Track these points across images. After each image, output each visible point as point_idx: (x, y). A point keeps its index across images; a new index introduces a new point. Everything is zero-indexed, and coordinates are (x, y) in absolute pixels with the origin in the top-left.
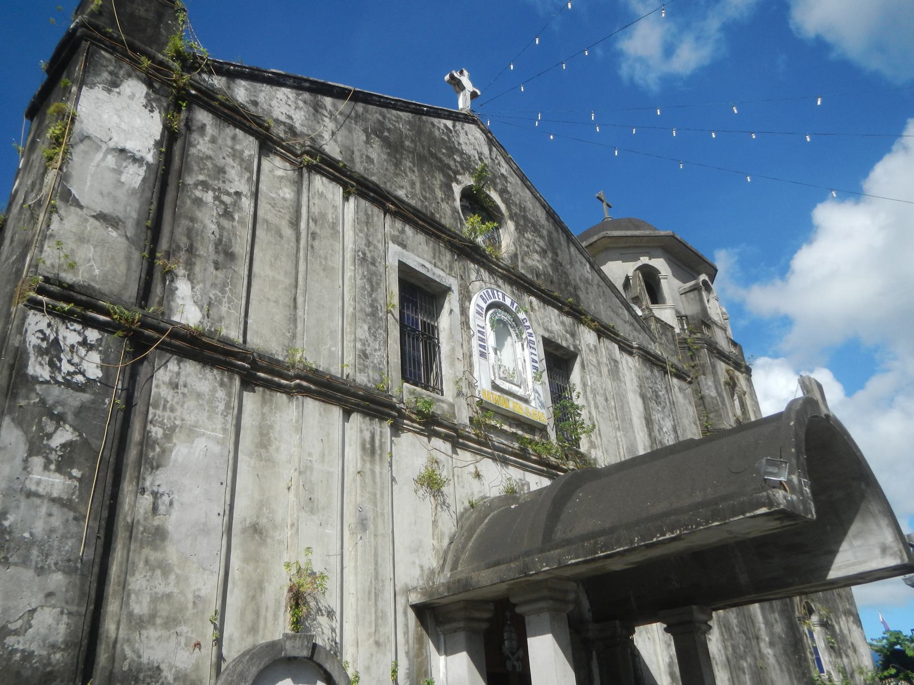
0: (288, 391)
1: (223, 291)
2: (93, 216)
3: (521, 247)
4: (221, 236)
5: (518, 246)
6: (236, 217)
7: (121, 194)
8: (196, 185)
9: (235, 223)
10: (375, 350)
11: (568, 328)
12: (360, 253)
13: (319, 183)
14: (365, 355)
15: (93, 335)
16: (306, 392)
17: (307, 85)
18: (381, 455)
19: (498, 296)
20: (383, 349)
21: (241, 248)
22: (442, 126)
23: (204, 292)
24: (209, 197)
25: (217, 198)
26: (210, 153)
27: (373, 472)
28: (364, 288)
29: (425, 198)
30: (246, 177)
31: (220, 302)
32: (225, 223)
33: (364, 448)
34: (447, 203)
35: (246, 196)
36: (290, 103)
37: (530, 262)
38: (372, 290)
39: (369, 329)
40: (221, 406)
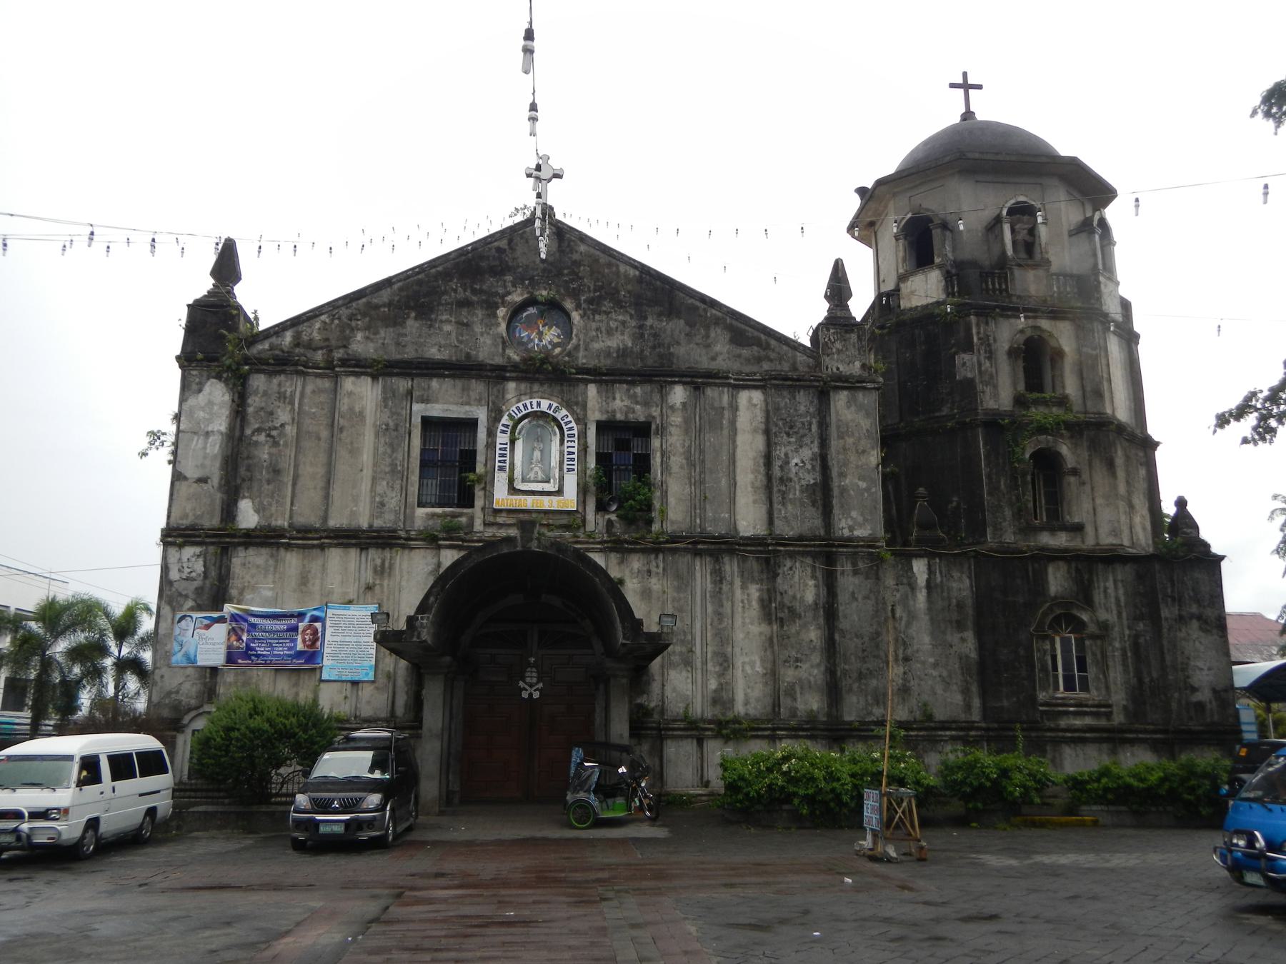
0: (322, 547)
1: (272, 497)
2: (196, 482)
3: (586, 335)
4: (271, 460)
5: (582, 336)
6: (281, 443)
7: (208, 462)
8: (253, 433)
9: (281, 448)
10: (392, 498)
11: (639, 399)
12: (384, 427)
13: (349, 383)
14: (382, 504)
15: (197, 550)
16: (330, 546)
17: (340, 302)
18: (390, 575)
19: (531, 405)
20: (399, 495)
21: (286, 463)
22: (494, 250)
23: (261, 503)
24: (262, 438)
25: (269, 436)
26: (263, 405)
27: (382, 585)
28: (384, 453)
29: (461, 342)
30: (288, 409)
31: (270, 505)
32: (274, 450)
33: (375, 571)
34: (488, 334)
35: (288, 424)
36: (327, 327)
37: (596, 346)
38: (393, 452)
39: (388, 483)
40: (272, 569)
